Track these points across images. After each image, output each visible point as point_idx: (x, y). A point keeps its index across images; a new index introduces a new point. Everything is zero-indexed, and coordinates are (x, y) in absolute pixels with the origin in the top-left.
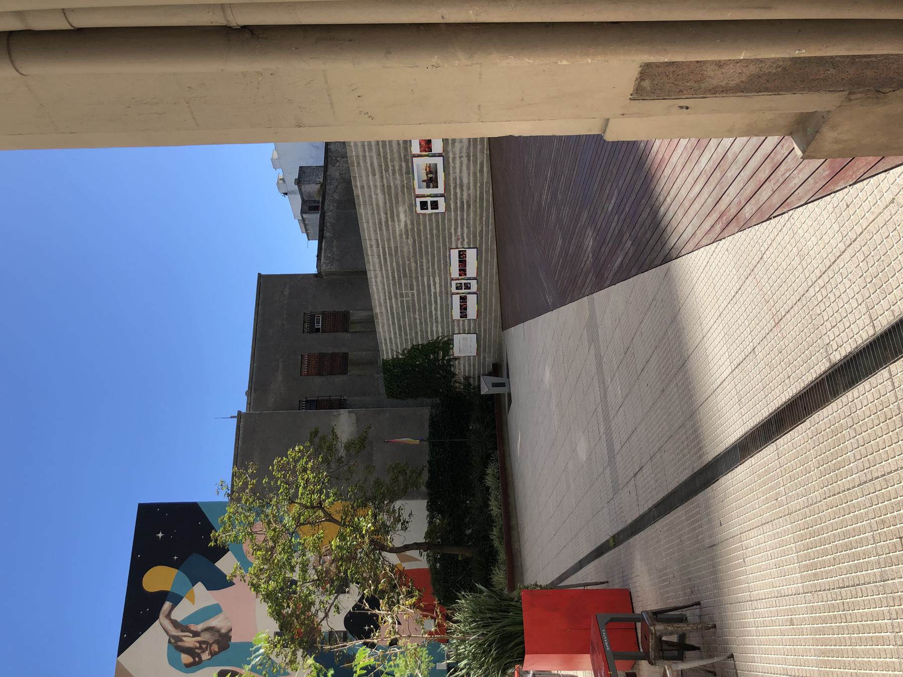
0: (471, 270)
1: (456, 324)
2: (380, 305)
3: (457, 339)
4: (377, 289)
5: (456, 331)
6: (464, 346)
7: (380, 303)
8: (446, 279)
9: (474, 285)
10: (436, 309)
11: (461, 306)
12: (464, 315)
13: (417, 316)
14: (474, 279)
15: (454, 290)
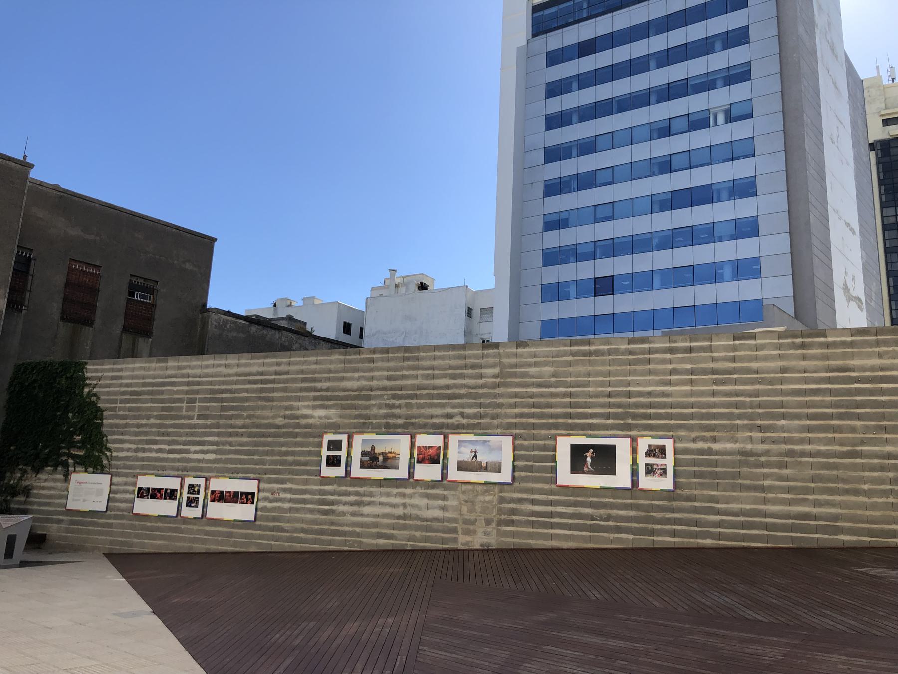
0: (217, 511)
1: (130, 480)
2: (179, 368)
3: (104, 480)
4: (207, 367)
5: (115, 480)
6: (88, 491)
7: (185, 368)
8: (209, 470)
9: (194, 513)
10: (160, 451)
11: (159, 490)
12: (142, 493)
13: (152, 421)
14: (204, 514)
15: (189, 481)
